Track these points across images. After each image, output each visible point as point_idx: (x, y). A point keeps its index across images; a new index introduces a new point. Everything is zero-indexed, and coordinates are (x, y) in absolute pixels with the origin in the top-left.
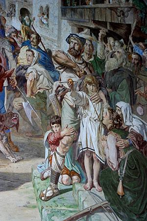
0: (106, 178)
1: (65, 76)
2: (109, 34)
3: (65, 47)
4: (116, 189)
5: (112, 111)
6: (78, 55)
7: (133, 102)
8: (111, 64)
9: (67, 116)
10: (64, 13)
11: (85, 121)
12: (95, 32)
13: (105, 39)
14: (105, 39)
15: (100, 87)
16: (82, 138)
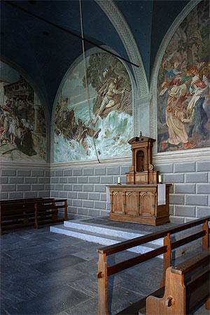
0: (17, 141)
1: (5, 112)
2: (20, 99)
3: (5, 104)
4: (20, 143)
5: (20, 122)
6: (9, 106)
7: (27, 119)
8: (20, 108)
9: (5, 124)
10: (5, 94)
11: (11, 125)
12: (15, 99)
13: (18, 100)
14: (18, 100)
15: (16, 115)
16: (10, 130)
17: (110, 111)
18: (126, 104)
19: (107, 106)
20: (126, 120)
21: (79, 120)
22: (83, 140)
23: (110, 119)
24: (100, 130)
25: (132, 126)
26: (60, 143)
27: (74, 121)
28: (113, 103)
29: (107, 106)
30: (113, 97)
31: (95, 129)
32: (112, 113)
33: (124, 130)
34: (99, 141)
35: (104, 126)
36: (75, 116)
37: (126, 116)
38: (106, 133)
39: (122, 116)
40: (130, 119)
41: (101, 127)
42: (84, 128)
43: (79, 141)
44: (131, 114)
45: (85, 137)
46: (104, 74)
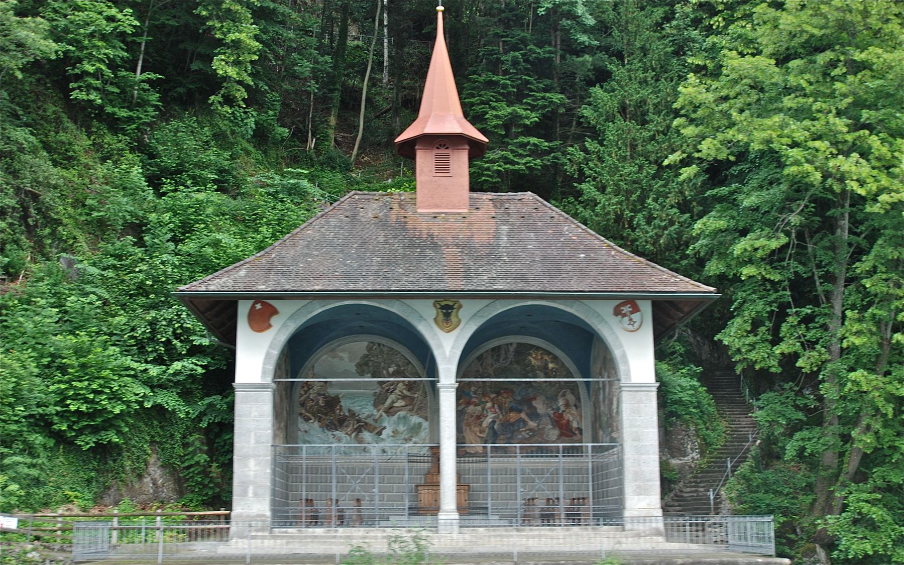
17: (399, 411)
18: (420, 409)
19: (395, 405)
20: (420, 424)
21: (349, 411)
22: (357, 435)
23: (399, 418)
24: (385, 428)
25: (427, 430)
26: (312, 432)
27: (341, 410)
28: (403, 403)
29: (395, 405)
30: (404, 397)
31: (377, 425)
32: (402, 413)
33: (417, 433)
34: (383, 440)
35: (389, 425)
36: (342, 404)
37: (420, 420)
38: (393, 432)
39: (415, 419)
40: (425, 424)
41: (385, 424)
42: (359, 421)
43: (350, 435)
44: (426, 419)
45: (360, 431)
46: (391, 370)
